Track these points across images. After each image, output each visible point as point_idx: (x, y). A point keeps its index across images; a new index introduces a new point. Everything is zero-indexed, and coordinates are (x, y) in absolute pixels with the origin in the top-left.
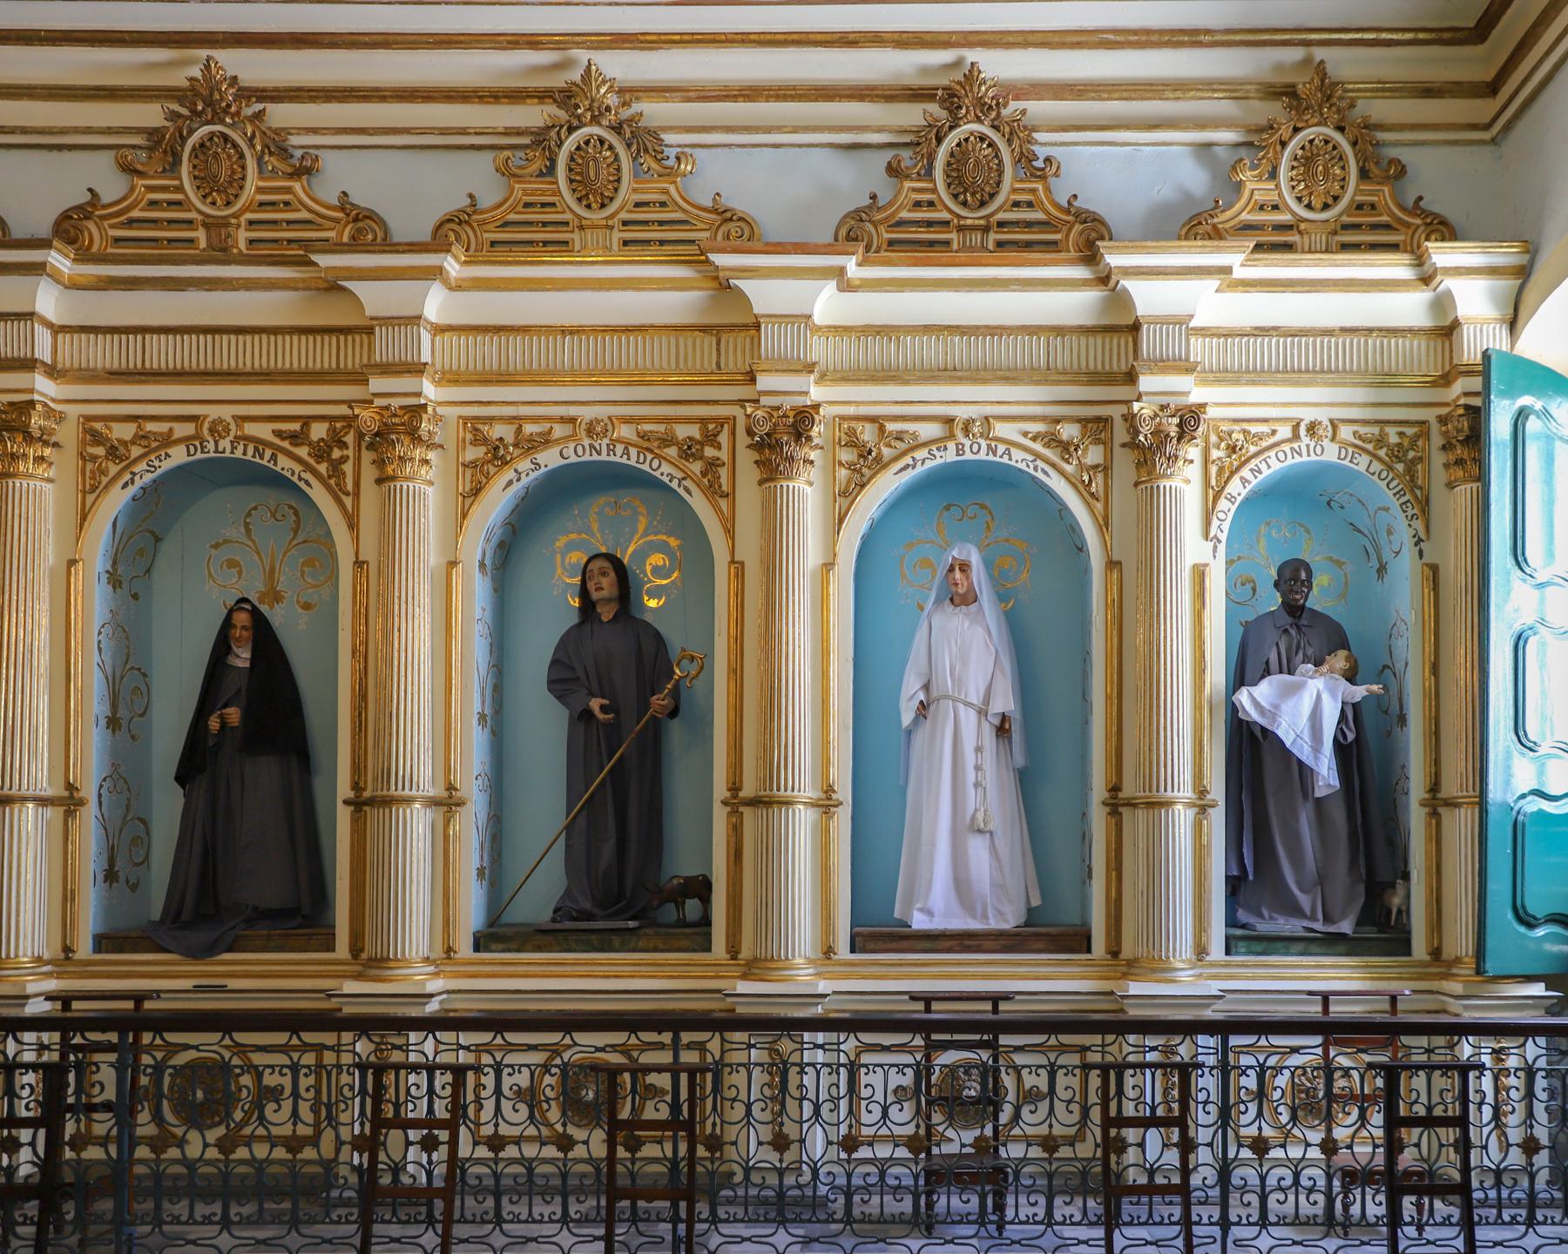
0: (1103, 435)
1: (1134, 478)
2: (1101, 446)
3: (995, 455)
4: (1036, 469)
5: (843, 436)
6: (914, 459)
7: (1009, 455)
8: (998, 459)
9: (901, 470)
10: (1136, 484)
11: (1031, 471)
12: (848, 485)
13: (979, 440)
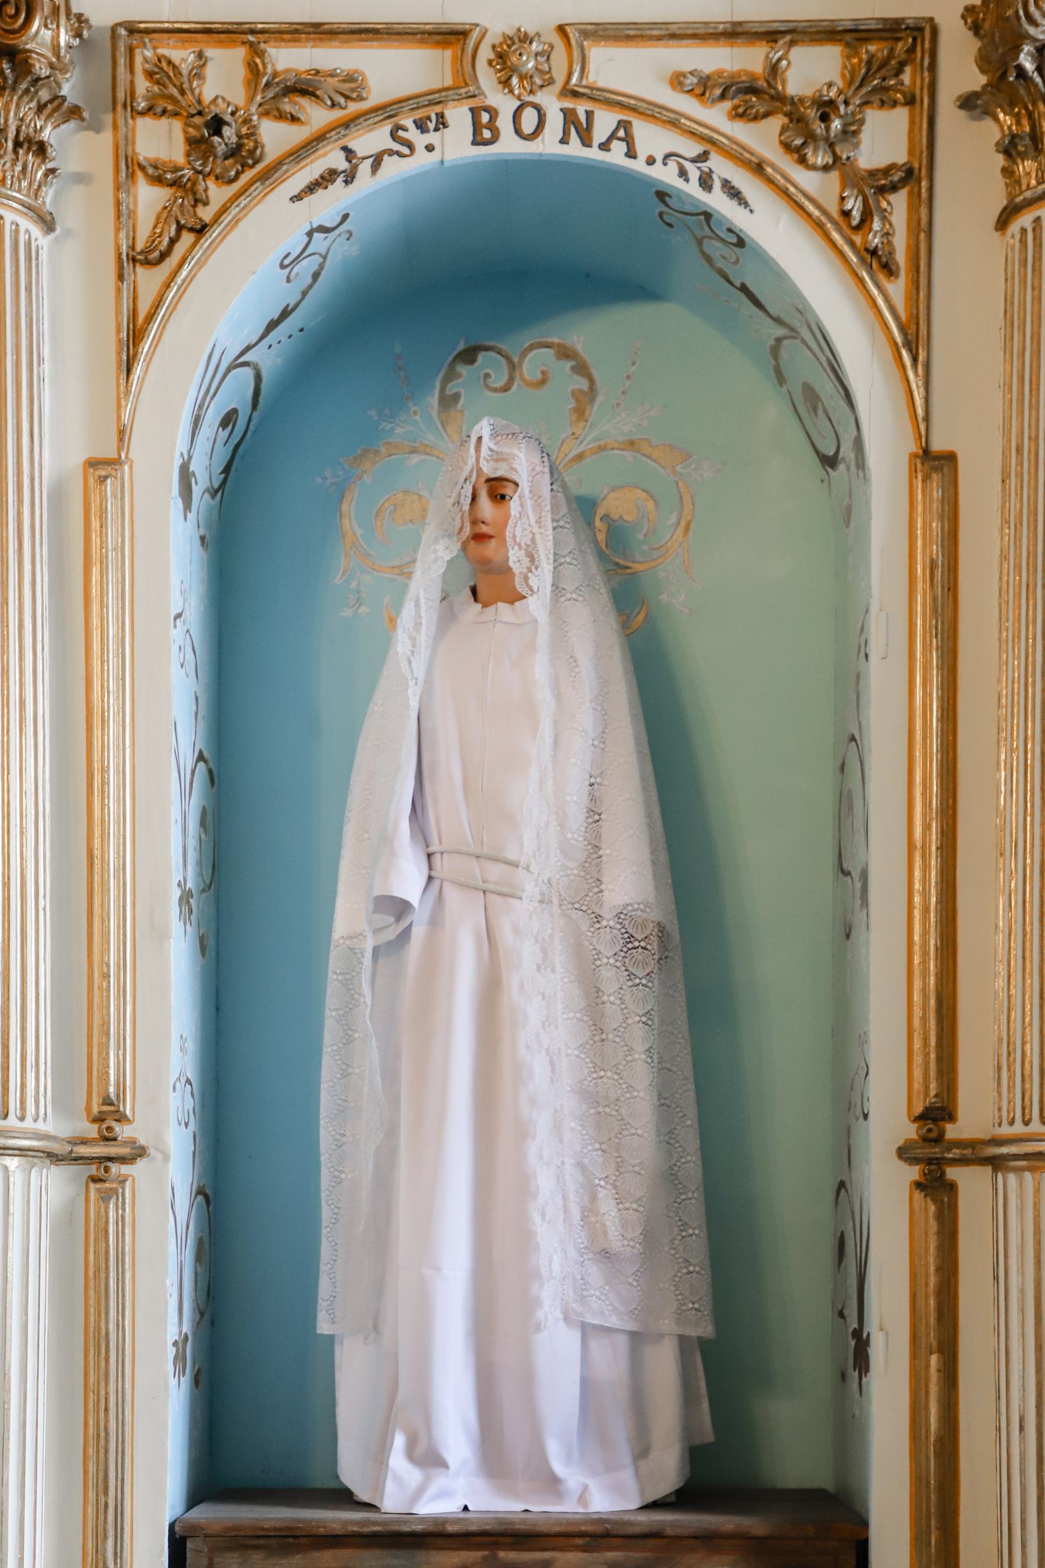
0: (906, 77)
1: (999, 201)
2: (901, 115)
3: (586, 142)
4: (705, 182)
5: (142, 85)
6: (349, 152)
7: (629, 141)
8: (594, 154)
9: (311, 188)
10: (1003, 222)
11: (692, 188)
12: (154, 237)
13: (539, 98)
